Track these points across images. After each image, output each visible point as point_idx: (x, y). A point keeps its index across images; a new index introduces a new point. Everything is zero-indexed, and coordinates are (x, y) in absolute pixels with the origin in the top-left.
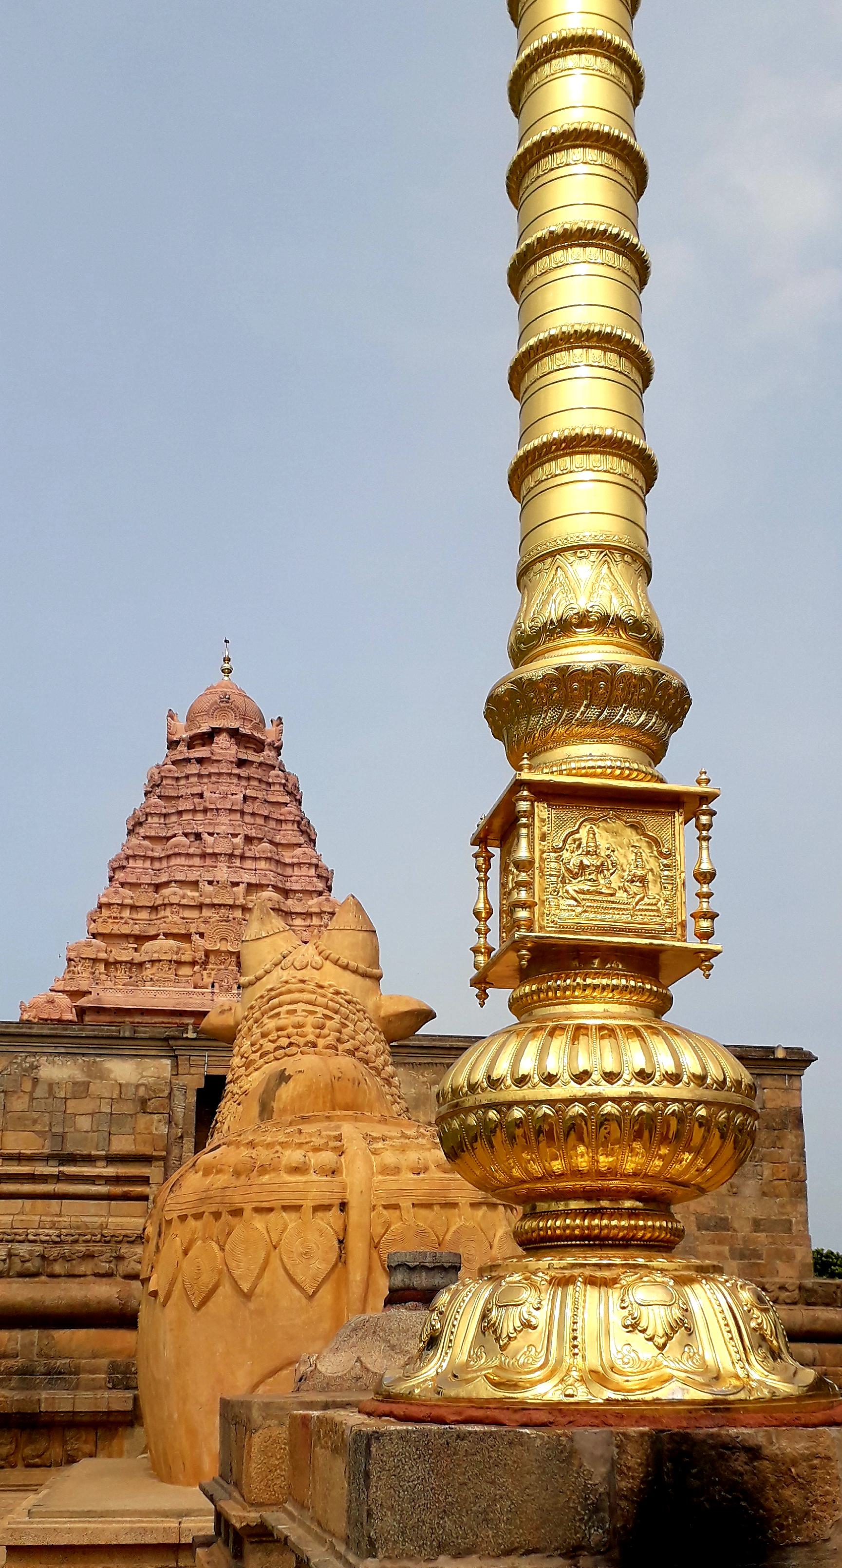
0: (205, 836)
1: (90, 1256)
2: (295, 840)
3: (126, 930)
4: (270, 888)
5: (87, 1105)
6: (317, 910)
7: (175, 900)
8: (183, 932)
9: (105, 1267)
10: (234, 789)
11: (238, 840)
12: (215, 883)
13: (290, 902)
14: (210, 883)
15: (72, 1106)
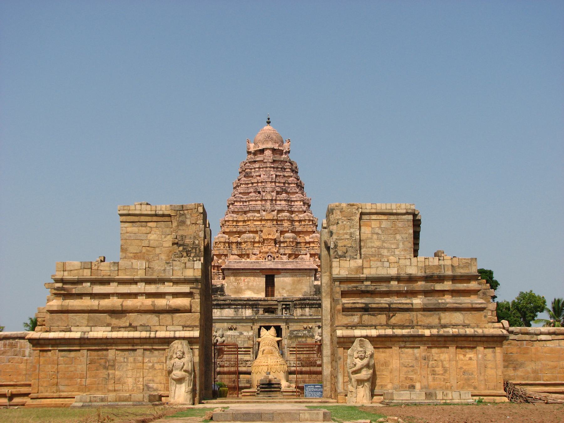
0: (261, 193)
1: (242, 363)
2: (295, 191)
3: (235, 230)
4: (286, 211)
5: (240, 339)
6: (304, 219)
7: (251, 218)
8: (255, 230)
9: (244, 365)
10: (272, 173)
11: (274, 194)
12: (266, 211)
13: (293, 215)
14: (264, 211)
15: (238, 339)
